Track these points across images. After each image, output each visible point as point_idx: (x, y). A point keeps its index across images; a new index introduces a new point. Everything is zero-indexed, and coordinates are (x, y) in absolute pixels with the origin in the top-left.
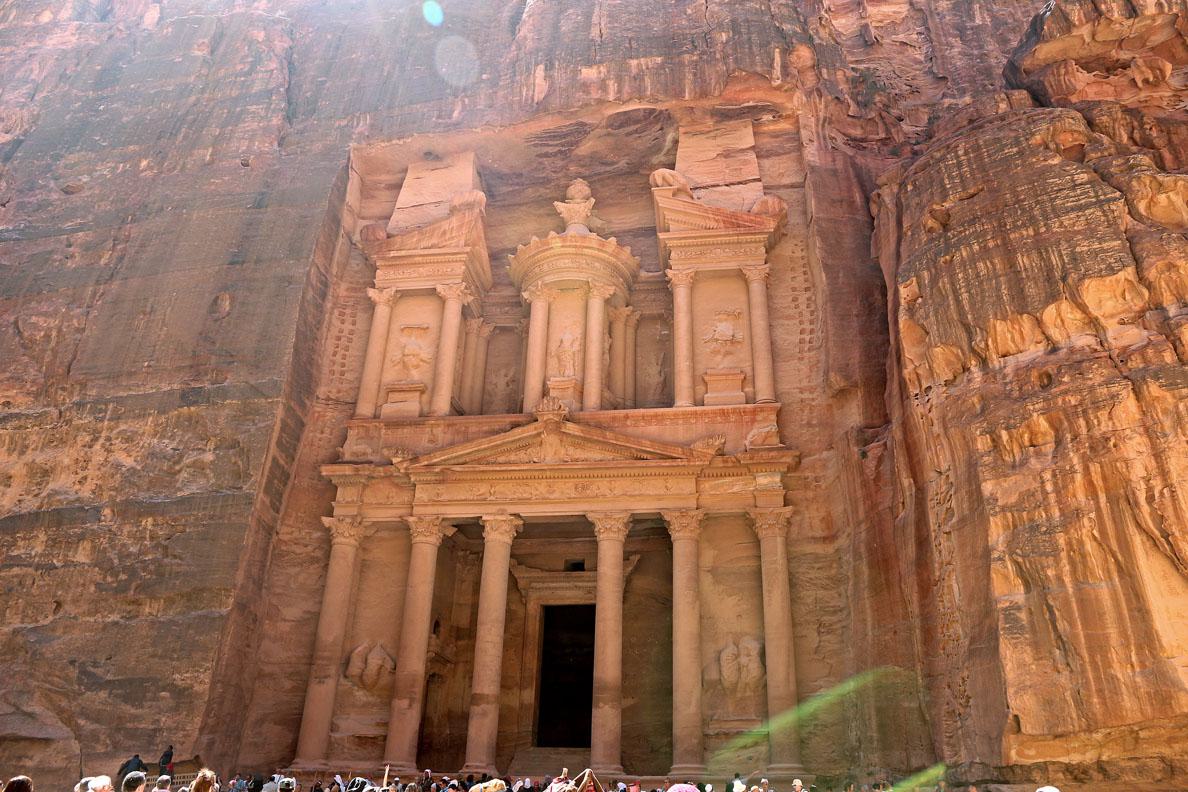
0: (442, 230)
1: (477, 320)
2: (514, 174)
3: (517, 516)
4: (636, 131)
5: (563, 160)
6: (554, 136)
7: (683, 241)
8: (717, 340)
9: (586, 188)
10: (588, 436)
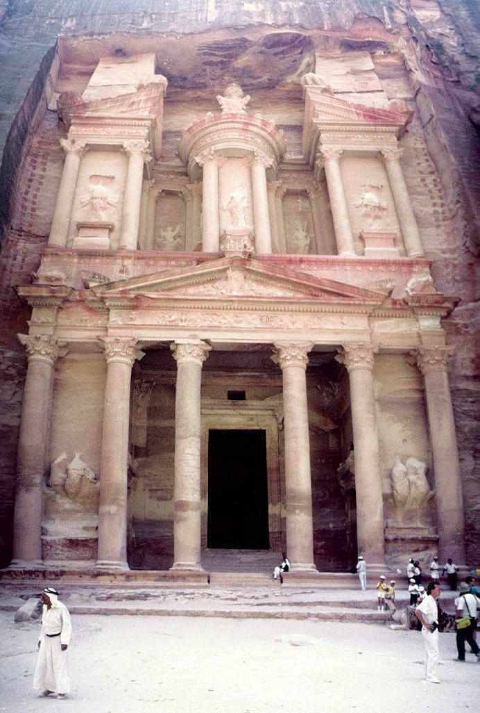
0: (132, 101)
1: (149, 182)
2: (180, 77)
3: (207, 341)
4: (282, 52)
5: (221, 70)
6: (221, 48)
7: (331, 127)
8: (366, 205)
9: (240, 90)
10: (271, 273)
